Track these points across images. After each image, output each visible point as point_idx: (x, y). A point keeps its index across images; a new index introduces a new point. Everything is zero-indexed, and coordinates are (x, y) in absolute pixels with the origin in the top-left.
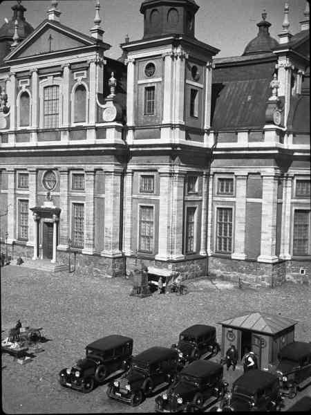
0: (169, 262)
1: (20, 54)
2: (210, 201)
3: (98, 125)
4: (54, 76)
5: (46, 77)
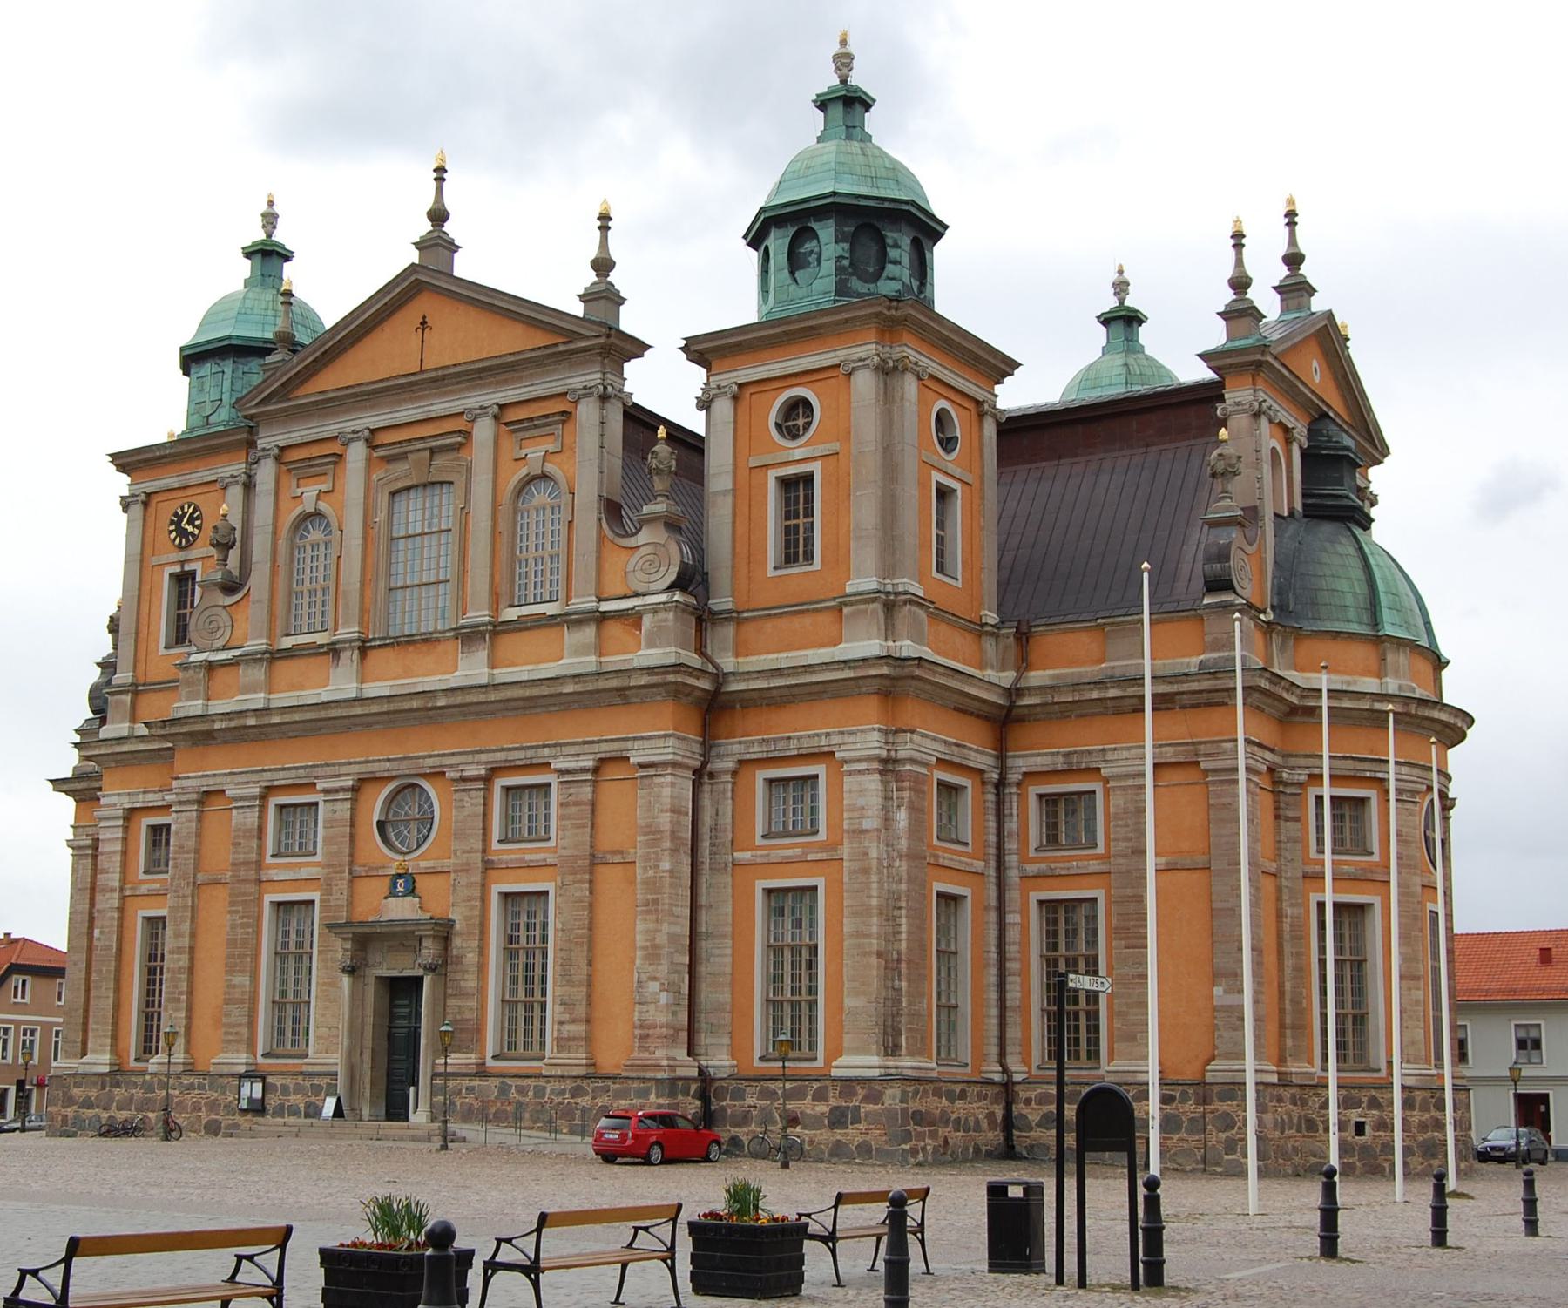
0: (887, 1079)
1: (302, 383)
2: (1013, 875)
3: (605, 606)
5: (403, 457)
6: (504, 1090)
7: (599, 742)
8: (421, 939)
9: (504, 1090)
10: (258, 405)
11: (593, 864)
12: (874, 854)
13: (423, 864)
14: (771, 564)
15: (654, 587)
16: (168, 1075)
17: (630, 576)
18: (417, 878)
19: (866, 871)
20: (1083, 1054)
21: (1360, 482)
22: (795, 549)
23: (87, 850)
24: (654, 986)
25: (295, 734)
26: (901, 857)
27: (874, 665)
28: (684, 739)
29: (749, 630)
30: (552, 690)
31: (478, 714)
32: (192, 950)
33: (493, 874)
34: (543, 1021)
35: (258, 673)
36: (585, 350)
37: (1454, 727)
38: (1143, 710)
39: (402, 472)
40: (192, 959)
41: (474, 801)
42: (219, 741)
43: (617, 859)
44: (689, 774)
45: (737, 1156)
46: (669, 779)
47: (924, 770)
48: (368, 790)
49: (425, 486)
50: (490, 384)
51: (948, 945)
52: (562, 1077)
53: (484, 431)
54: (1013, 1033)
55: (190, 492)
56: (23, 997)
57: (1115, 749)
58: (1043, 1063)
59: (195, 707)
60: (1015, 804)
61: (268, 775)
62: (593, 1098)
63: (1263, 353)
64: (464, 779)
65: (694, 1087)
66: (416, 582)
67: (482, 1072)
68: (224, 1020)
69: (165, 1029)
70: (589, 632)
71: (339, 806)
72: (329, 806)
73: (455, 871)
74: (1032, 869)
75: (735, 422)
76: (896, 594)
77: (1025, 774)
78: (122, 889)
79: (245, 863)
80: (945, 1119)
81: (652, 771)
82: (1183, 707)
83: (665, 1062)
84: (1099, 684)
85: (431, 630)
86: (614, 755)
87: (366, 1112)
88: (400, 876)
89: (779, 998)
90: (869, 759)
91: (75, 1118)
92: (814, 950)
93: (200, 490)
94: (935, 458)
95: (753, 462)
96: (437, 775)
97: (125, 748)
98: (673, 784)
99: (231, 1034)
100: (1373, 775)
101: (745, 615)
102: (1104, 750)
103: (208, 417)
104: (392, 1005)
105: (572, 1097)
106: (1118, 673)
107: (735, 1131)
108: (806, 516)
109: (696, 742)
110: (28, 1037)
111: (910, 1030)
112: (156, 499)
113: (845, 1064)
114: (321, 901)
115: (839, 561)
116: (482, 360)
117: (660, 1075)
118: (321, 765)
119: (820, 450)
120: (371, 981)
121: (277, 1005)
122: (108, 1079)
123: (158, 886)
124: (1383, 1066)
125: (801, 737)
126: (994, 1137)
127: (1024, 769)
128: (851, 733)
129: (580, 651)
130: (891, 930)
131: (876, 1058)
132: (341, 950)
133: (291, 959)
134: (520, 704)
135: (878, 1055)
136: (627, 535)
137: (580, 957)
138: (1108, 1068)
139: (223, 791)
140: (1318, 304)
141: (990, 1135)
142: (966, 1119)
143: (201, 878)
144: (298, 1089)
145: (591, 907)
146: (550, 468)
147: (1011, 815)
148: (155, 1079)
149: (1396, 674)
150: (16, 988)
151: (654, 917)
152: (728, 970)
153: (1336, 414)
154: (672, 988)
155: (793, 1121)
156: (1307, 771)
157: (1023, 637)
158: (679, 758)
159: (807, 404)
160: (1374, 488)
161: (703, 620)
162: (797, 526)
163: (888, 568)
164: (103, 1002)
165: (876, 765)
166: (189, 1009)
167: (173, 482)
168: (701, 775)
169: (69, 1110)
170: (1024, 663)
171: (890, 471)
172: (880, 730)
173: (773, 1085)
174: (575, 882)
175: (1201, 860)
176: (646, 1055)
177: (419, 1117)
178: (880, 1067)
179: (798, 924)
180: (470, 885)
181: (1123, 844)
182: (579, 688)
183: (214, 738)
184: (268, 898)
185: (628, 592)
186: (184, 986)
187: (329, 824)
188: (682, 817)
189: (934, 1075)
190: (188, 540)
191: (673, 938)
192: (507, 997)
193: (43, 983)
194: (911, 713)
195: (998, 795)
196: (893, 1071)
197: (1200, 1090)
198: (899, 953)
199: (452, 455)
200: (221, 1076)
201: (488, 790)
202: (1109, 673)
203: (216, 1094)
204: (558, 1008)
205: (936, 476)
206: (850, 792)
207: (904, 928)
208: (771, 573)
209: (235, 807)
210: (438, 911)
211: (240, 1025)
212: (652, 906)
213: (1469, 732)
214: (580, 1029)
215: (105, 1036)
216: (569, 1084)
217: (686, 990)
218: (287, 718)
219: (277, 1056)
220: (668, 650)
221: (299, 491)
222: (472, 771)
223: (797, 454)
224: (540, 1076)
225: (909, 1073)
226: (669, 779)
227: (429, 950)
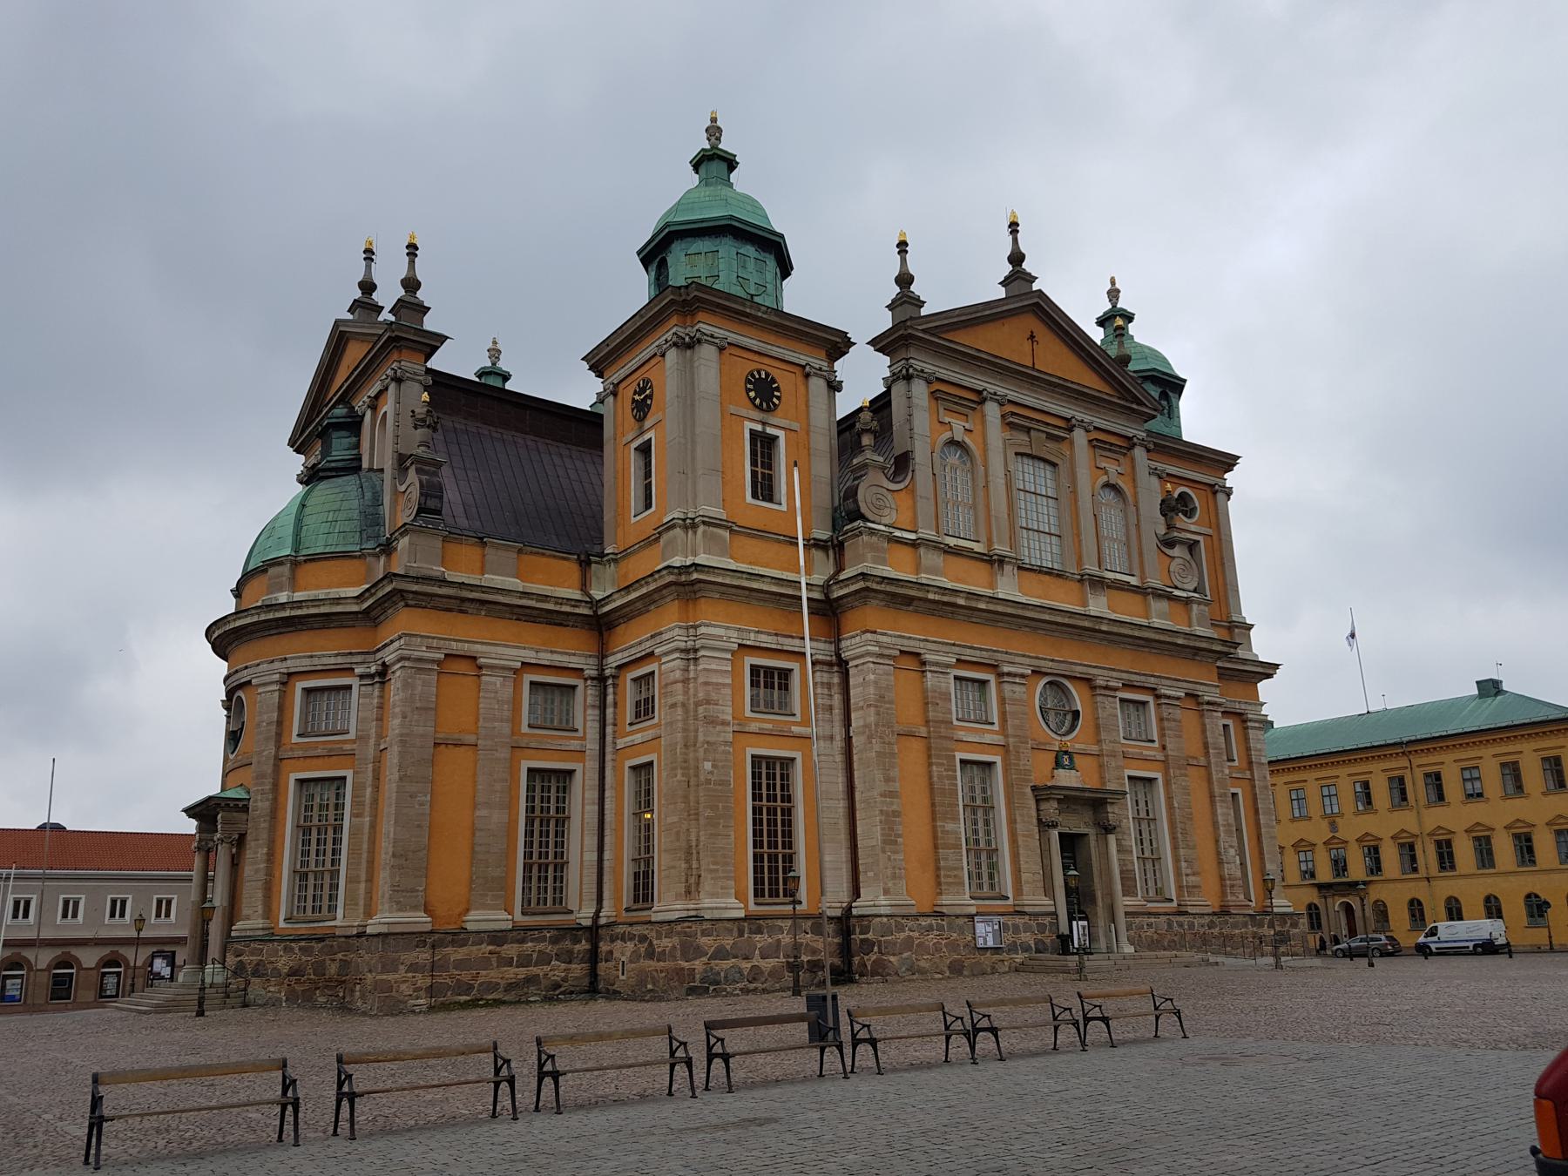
1: (948, 331)
4: (1050, 437)
5: (1028, 430)
9: (1170, 925)
10: (924, 331)
13: (1077, 746)
15: (1186, 587)
25: (978, 620)
30: (1168, 639)
31: (1110, 641)
42: (911, 608)
61: (956, 649)
71: (1017, 688)
73: (1107, 756)
79: (942, 722)
88: (1066, 752)
91: (705, 971)
99: (949, 876)
122: (746, 924)
123: (770, 726)
144: (1027, 929)
169: (697, 962)
174: (1182, 775)
176: (1234, 898)
184: (959, 756)
200: (957, 916)
203: (955, 935)
215: (728, 878)
216: (1207, 920)
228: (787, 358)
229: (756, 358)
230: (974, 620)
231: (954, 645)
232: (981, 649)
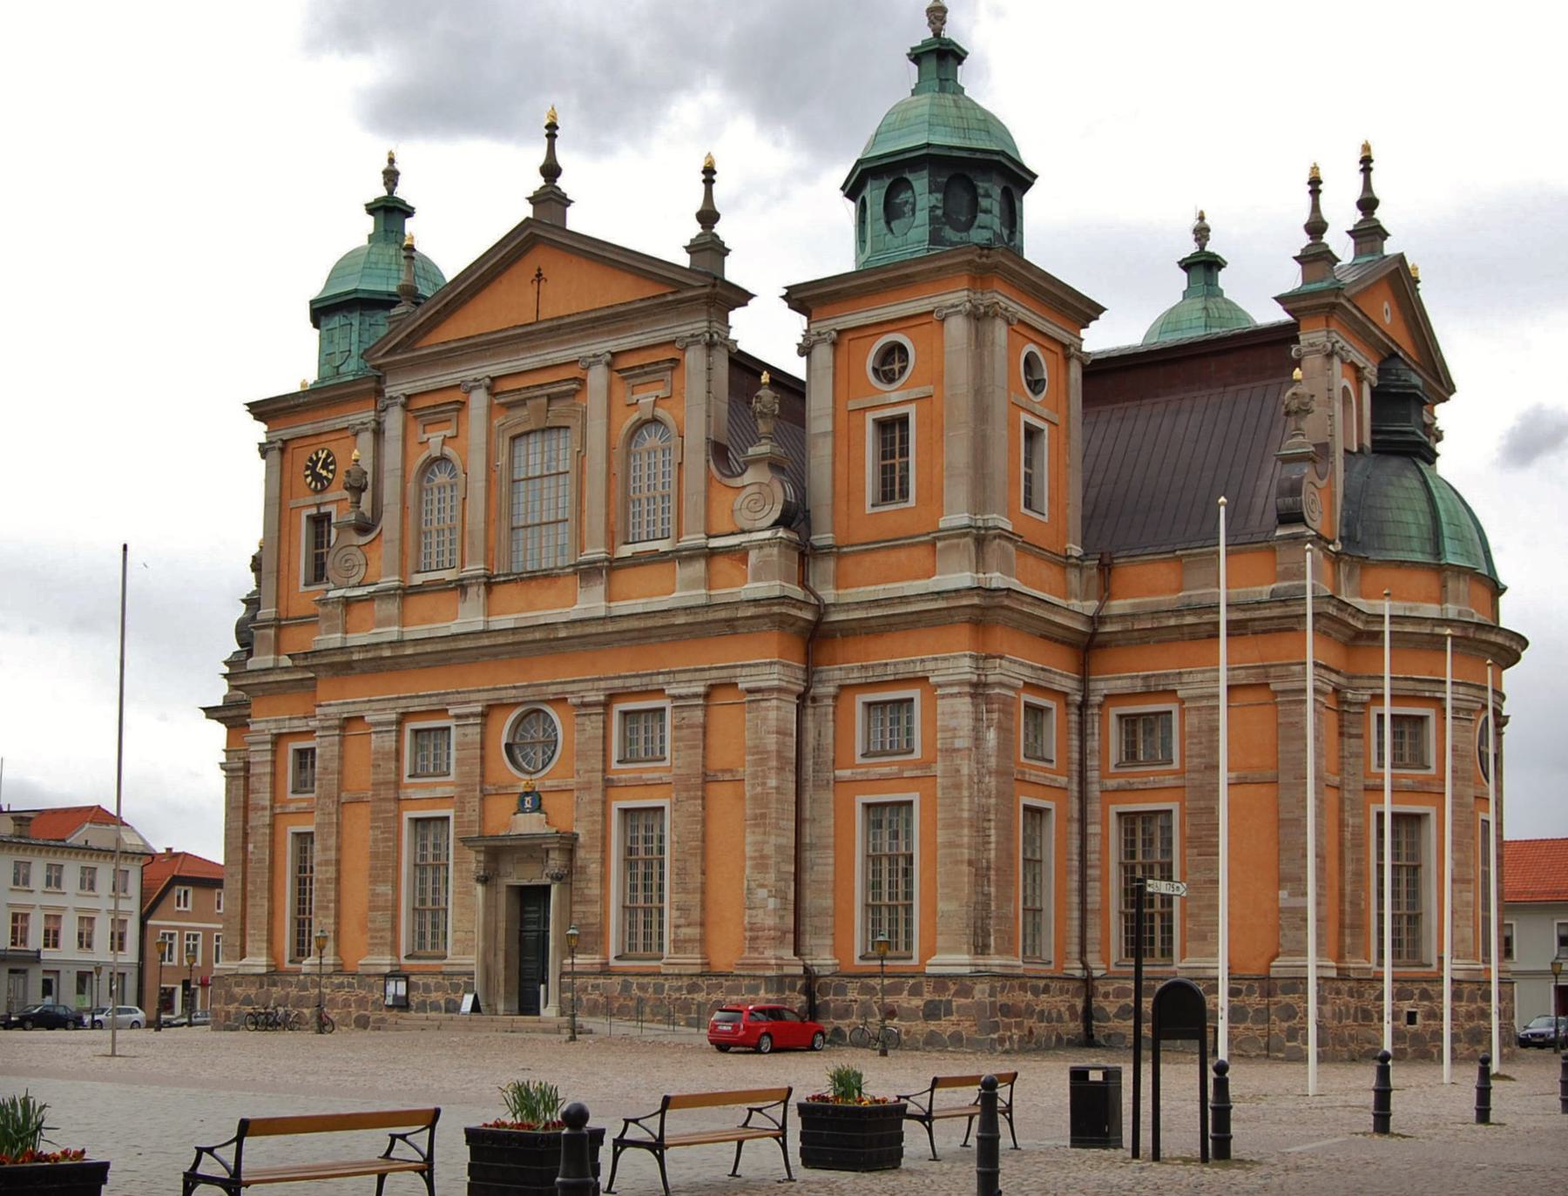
0: (977, 976)
2: (1094, 790)
3: (714, 543)
6: (626, 987)
7: (710, 669)
8: (547, 851)
9: (626, 987)
11: (705, 782)
12: (965, 771)
13: (548, 783)
14: (869, 501)
15: (759, 524)
16: (320, 975)
17: (737, 514)
18: (543, 795)
19: (958, 787)
20: (1157, 953)
21: (1426, 419)
22: (891, 487)
23: (238, 771)
24: (763, 893)
26: (990, 773)
27: (965, 596)
28: (788, 666)
29: (848, 563)
31: (596, 644)
32: (338, 862)
33: (613, 792)
34: (661, 925)
35: (391, 608)
36: (691, 299)
37: (1510, 649)
38: (1217, 636)
39: (521, 418)
40: (338, 871)
41: (593, 725)
42: (358, 670)
43: (728, 777)
44: (794, 699)
45: (840, 1045)
46: (774, 703)
47: (1012, 694)
48: (497, 715)
49: (543, 430)
50: (603, 334)
51: (1034, 852)
52: (680, 975)
53: (597, 378)
54: (1093, 933)
55: (324, 438)
56: (185, 905)
57: (1191, 672)
58: (1121, 960)
59: (334, 639)
60: (1097, 725)
61: (403, 703)
62: (708, 994)
63: (1337, 296)
64: (584, 705)
65: (799, 984)
66: (537, 521)
67: (605, 971)
68: (369, 925)
69: (316, 933)
70: (699, 567)
71: (469, 730)
72: (461, 730)
73: (578, 789)
74: (1111, 783)
75: (835, 367)
76: (987, 529)
77: (1106, 696)
78: (272, 808)
79: (382, 784)
80: (1030, 1012)
81: (759, 696)
82: (1255, 633)
83: (773, 962)
84: (1177, 612)
85: (551, 566)
86: (727, 681)
87: (501, 1007)
88: (527, 794)
89: (878, 903)
90: (960, 683)
92: (909, 859)
93: (333, 437)
94: (1024, 400)
95: (852, 405)
96: (559, 701)
97: (271, 678)
98: (778, 708)
100: (1431, 694)
101: (845, 550)
102: (1180, 673)
103: (338, 367)
104: (522, 911)
105: (689, 993)
106: (1195, 601)
107: (837, 1023)
108: (901, 456)
109: (799, 668)
110: (191, 942)
111: (996, 931)
112: (292, 445)
113: (938, 962)
114: (456, 817)
115: (933, 498)
116: (595, 310)
117: (769, 973)
118: (453, 693)
119: (915, 392)
120: (504, 889)
121: (418, 912)
123: (304, 804)
124: (1435, 962)
125: (898, 663)
126: (1074, 1027)
127: (1105, 692)
128: (945, 659)
129: (691, 584)
130: (980, 840)
131: (967, 957)
132: (474, 861)
133: (430, 870)
134: (635, 634)
135: (969, 953)
136: (734, 475)
137: (694, 867)
138: (1183, 965)
139: (363, 717)
140: (1390, 248)
141: (1072, 1025)
142: (1049, 1013)
143: (345, 797)
144: (438, 987)
145: (704, 822)
146: (660, 412)
147: (1093, 734)
148: (309, 979)
149: (1456, 601)
150: (179, 897)
151: (762, 829)
152: (830, 877)
153: (1406, 353)
154: (779, 894)
155: (891, 1013)
156: (1370, 692)
157: (1106, 568)
158: (784, 684)
159: (902, 349)
160: (1440, 424)
161: (805, 555)
162: (893, 466)
163: (979, 504)
164: (259, 909)
165: (967, 689)
166: (338, 916)
167: (306, 429)
168: (804, 700)
170: (1106, 593)
171: (981, 411)
172: (971, 656)
173: (872, 982)
174: (688, 798)
175: (1269, 774)
176: (756, 955)
177: (549, 1012)
178: (970, 965)
179: (895, 835)
180: (592, 802)
181: (1196, 761)
182: (690, 619)
183: (352, 669)
184: (407, 815)
185: (735, 530)
186: (332, 895)
187: (462, 746)
188: (787, 739)
189: (1020, 971)
190: (323, 485)
191: (779, 849)
192: (628, 903)
193: (204, 894)
194: (1000, 639)
195: (1080, 715)
196: (982, 968)
197: (1265, 983)
198: (988, 861)
199: (570, 401)
200: (368, 976)
201: (607, 715)
202: (1186, 601)
204: (675, 913)
205: (1025, 417)
206: (943, 713)
207: (993, 839)
208: (869, 510)
209: (375, 732)
210: (563, 824)
211: (383, 930)
212: (760, 820)
213: (1523, 654)
214: (694, 932)
215: (262, 941)
216: (686, 982)
217: (791, 896)
218: (420, 649)
219: (419, 958)
220: (773, 583)
221: (425, 437)
222: (591, 697)
223: (894, 397)
224: (660, 974)
225: (997, 970)
226: (774, 703)
227: (556, 861)
228: (338, 427)
229: (314, 440)
230: (424, 664)
231: (399, 698)
232: (430, 696)
